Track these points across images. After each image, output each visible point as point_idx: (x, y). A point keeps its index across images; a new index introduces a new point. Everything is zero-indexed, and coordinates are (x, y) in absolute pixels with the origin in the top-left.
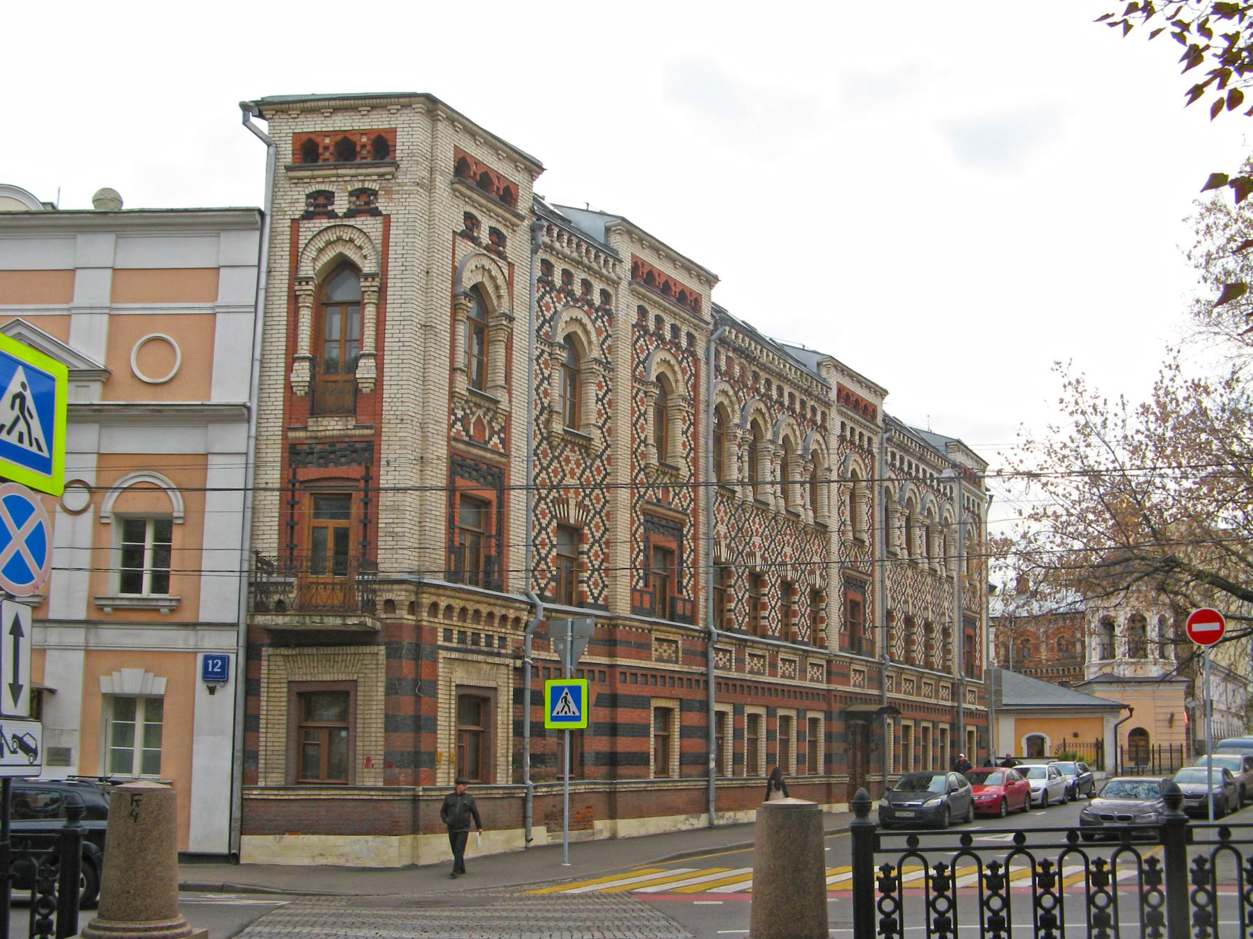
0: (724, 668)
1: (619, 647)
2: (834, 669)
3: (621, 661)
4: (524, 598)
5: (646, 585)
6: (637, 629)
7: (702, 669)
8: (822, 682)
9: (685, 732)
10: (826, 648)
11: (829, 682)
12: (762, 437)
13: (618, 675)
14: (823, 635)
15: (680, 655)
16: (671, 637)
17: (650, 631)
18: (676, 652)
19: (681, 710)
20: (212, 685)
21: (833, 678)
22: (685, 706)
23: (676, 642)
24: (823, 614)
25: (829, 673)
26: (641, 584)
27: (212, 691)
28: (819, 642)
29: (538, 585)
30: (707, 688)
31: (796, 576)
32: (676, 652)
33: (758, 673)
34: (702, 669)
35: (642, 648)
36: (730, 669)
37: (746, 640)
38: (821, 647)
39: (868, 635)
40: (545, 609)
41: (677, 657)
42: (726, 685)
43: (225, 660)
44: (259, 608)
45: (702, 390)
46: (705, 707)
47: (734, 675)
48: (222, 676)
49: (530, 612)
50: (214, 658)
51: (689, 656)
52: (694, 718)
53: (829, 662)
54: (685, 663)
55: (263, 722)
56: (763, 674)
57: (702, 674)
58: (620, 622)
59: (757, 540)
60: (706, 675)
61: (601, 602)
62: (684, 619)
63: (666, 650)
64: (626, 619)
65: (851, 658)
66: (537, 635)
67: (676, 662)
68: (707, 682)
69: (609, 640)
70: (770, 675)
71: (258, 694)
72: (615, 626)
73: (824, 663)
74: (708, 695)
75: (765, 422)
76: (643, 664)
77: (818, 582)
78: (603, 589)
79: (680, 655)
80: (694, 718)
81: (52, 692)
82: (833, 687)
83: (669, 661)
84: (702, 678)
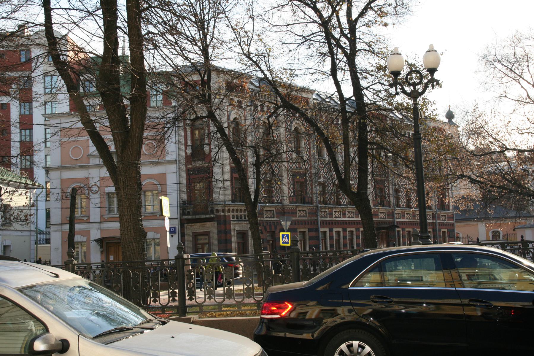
0: (325, 217)
6: (291, 208)
7: (316, 218)
17: (296, 208)
18: (306, 214)
30: (318, 224)
32: (306, 214)
33: (339, 217)
34: (316, 218)
41: (306, 215)
42: (325, 223)
43: (175, 228)
46: (317, 230)
47: (329, 219)
48: (175, 232)
52: (313, 234)
54: (309, 217)
56: (341, 217)
62: (308, 203)
63: (302, 214)
68: (317, 222)
70: (343, 217)
72: (284, 208)
80: (313, 234)
83: (303, 217)
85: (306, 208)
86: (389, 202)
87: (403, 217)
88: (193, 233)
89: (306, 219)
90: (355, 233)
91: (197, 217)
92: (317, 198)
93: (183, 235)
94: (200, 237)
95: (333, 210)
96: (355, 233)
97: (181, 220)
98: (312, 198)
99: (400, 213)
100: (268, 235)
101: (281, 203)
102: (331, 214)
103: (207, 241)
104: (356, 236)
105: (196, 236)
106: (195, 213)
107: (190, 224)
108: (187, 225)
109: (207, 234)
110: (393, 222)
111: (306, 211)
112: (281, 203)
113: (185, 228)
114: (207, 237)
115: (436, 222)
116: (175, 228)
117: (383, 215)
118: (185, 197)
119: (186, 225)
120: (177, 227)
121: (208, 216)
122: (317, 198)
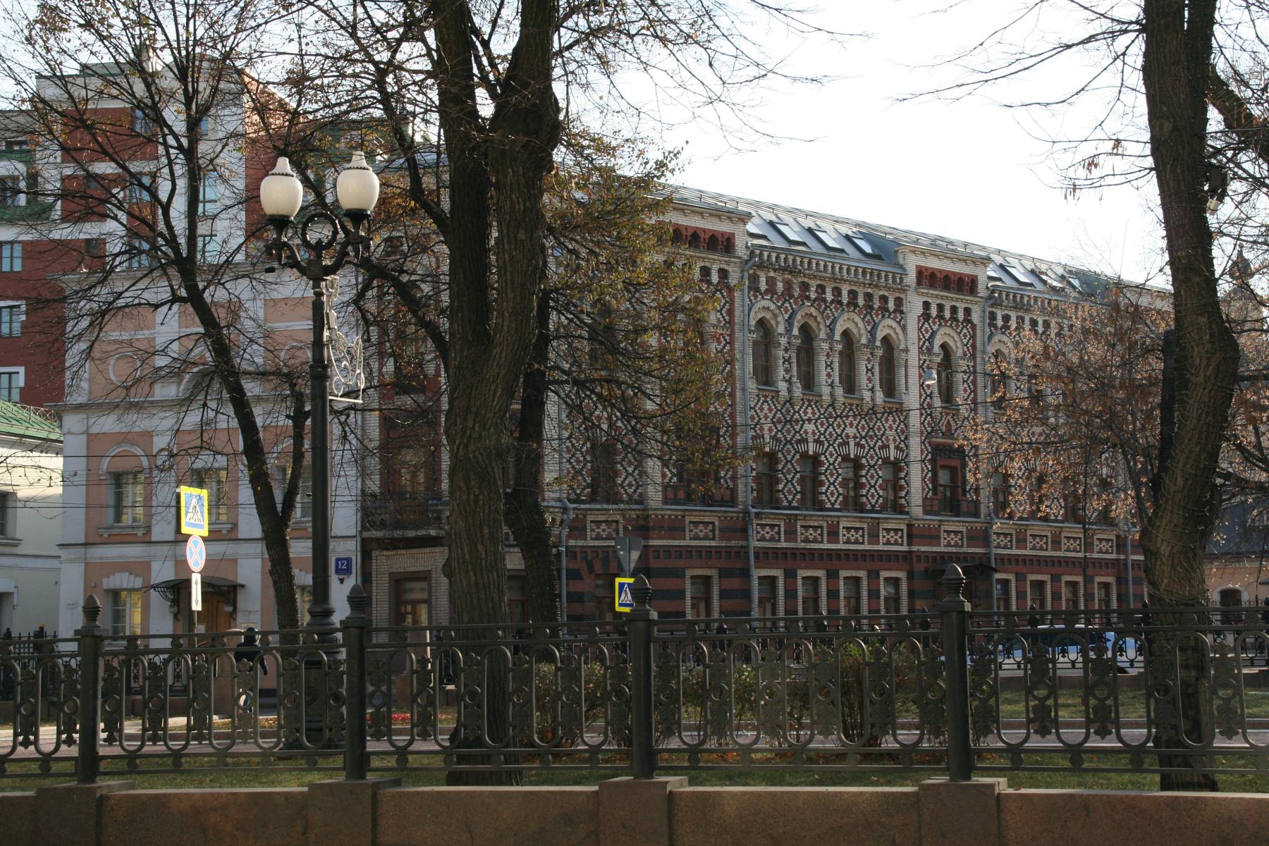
0: (772, 539)
1: (651, 533)
2: (915, 532)
3: (653, 543)
4: (558, 504)
5: (680, 480)
6: (670, 516)
7: (743, 543)
8: (902, 544)
9: (723, 594)
10: (907, 513)
11: (910, 544)
12: (817, 336)
13: (651, 554)
14: (903, 501)
15: (717, 533)
16: (707, 519)
17: (683, 517)
18: (713, 531)
19: (720, 577)
20: (341, 577)
21: (915, 540)
22: (723, 573)
23: (713, 523)
24: (902, 482)
25: (910, 536)
26: (675, 479)
27: (342, 581)
28: (898, 508)
29: (575, 492)
30: (748, 558)
31: (861, 452)
32: (713, 531)
33: (815, 541)
34: (743, 543)
35: (676, 528)
36: (779, 540)
37: (796, 515)
38: (901, 513)
39: (971, 496)
40: (574, 509)
41: (714, 535)
42: (766, 557)
43: (349, 560)
44: (364, 528)
45: (737, 313)
46: (745, 574)
47: (784, 544)
48: (348, 571)
49: (563, 513)
50: (341, 559)
51: (727, 532)
52: (734, 583)
53: (910, 526)
54: (721, 539)
55: (374, 600)
56: (822, 542)
57: (742, 547)
58: (650, 512)
59: (809, 427)
60: (747, 547)
61: (636, 497)
62: (722, 503)
63: (702, 531)
64: (662, 510)
65: (940, 521)
66: (572, 529)
67: (713, 539)
68: (747, 553)
69: (643, 527)
70: (829, 542)
71: (371, 582)
72: (648, 516)
73: (905, 528)
74: (748, 564)
75: (819, 323)
76: (682, 543)
77: (893, 454)
78: (637, 488)
79: (717, 533)
80: (734, 583)
81: (243, 586)
82: (915, 548)
83: (706, 538)
84: (743, 550)
85: (713, 516)
86: (977, 504)
87: (1021, 542)
88: (390, 574)
89: (713, 543)
90: (865, 583)
91: (395, 535)
92: (745, 492)
93: (366, 576)
94: (409, 585)
95: (799, 524)
96: (865, 583)
97: (364, 541)
98: (733, 492)
99: (1011, 535)
100: (600, 582)
101: (640, 502)
102: (791, 534)
103: (425, 596)
104: (869, 591)
105: (399, 582)
106: (398, 525)
107: (385, 553)
108: (377, 553)
109: (424, 577)
110: (987, 556)
111: (713, 523)
112: (640, 502)
113: (374, 561)
114: (424, 585)
115: (1126, 560)
116: (349, 560)
117: (954, 539)
118: (374, 485)
119: (375, 553)
120: (354, 558)
121: (421, 533)
122: (745, 492)
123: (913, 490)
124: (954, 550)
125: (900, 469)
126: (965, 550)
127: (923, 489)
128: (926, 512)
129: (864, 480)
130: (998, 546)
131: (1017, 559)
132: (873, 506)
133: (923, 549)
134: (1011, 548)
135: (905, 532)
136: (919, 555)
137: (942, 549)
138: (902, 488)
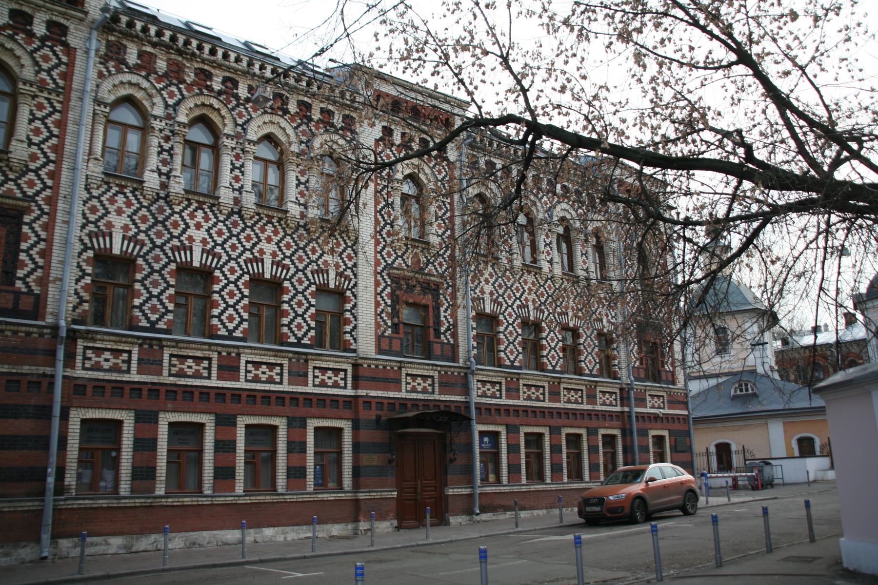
2: (361, 372)
123: (360, 325)
124: (420, 396)
125: (346, 300)
126: (436, 397)
127: (378, 325)
128: (380, 351)
129: (285, 307)
130: (484, 395)
131: (507, 410)
132: (299, 339)
133: (373, 393)
134: (501, 397)
135: (350, 373)
136: (368, 402)
137: (403, 395)
138: (347, 322)
